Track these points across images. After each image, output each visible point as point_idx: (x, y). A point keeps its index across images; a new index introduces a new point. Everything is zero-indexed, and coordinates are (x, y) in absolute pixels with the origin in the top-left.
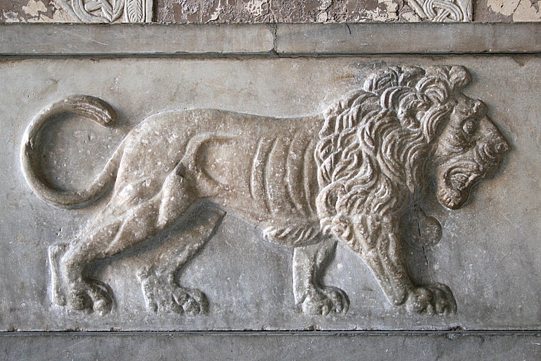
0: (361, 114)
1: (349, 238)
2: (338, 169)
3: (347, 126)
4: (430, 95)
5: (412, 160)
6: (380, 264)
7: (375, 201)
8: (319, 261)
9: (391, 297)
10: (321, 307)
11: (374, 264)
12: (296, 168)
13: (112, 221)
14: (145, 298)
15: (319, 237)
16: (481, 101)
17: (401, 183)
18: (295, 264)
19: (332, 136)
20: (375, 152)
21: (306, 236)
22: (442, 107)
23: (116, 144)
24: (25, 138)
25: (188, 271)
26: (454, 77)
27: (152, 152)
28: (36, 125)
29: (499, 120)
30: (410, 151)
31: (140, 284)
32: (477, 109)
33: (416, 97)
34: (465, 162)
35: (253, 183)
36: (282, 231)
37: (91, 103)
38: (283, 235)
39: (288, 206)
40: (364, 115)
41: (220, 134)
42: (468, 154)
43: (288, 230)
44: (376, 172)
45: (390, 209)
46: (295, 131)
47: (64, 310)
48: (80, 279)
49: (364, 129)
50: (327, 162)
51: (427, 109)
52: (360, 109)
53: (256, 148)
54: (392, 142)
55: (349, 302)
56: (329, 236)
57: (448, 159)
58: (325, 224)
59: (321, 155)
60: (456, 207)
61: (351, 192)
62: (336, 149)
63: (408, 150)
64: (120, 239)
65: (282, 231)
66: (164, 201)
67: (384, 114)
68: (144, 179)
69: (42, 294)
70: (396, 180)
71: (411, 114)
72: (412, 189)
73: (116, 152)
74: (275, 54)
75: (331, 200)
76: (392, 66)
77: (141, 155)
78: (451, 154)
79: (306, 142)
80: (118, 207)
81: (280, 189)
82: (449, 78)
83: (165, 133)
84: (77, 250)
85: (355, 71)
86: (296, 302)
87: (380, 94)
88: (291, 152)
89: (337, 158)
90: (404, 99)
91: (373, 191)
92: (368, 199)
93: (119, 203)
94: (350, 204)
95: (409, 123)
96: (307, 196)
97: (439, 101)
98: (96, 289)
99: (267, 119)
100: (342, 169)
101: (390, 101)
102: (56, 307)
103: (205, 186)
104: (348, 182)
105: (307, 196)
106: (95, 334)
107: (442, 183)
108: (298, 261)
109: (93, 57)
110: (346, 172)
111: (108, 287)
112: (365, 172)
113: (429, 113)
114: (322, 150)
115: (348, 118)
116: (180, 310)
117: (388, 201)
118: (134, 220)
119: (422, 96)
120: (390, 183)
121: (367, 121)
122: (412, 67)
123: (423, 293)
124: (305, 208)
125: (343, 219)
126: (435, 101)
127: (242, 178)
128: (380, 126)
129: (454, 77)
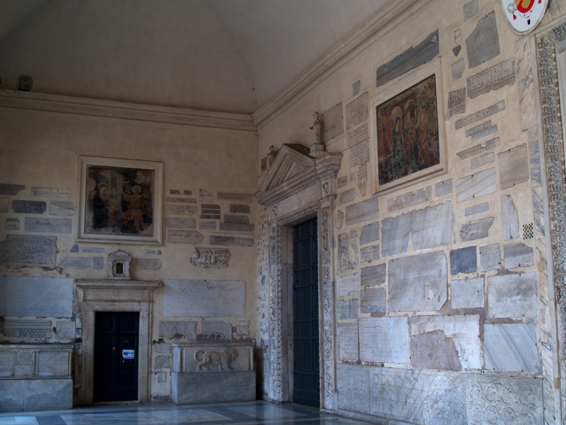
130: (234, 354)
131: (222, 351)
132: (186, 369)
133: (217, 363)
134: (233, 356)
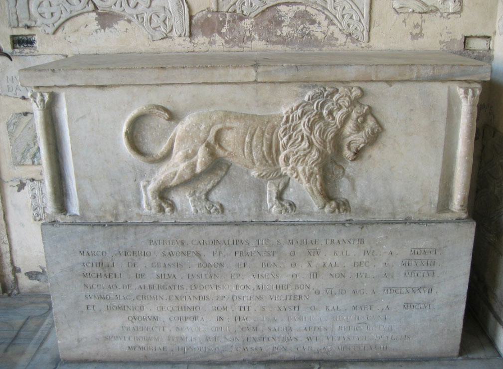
0: (303, 114)
1: (296, 177)
2: (290, 143)
3: (296, 120)
4: (341, 104)
5: (330, 138)
6: (312, 190)
7: (310, 159)
8: (281, 188)
9: (318, 205)
10: (281, 211)
11: (309, 190)
12: (268, 143)
13: (173, 170)
14: (191, 206)
15: (281, 176)
16: (368, 106)
17: (324, 150)
18: (268, 189)
19: (288, 126)
20: (311, 134)
21: (274, 175)
22: (347, 110)
23: (173, 130)
24: (124, 128)
25: (213, 193)
26: (354, 94)
27: (192, 135)
28: (130, 121)
29: (377, 115)
30: (329, 133)
31: (188, 200)
32: (366, 111)
33: (333, 104)
34: (358, 138)
35: (246, 151)
36: (261, 174)
37: (158, 109)
38: (262, 175)
39: (264, 162)
40: (305, 114)
41: (228, 124)
42: (360, 134)
43: (264, 173)
44: (311, 144)
45: (318, 163)
46: (268, 123)
47: (151, 212)
48: (158, 198)
49: (305, 122)
50: (285, 139)
51: (339, 111)
52: (303, 111)
53: (247, 132)
54: (320, 129)
55: (295, 207)
56: (285, 175)
57: (349, 136)
58: (284, 170)
59: (282, 135)
60: (352, 160)
61: (298, 155)
62: (290, 132)
63: (329, 131)
64: (177, 179)
65: (261, 174)
66: (199, 160)
67: (316, 114)
68: (188, 149)
69: (139, 205)
70: (321, 148)
71: (330, 113)
72: (330, 152)
73: (172, 134)
74: (256, 82)
75: (287, 159)
76: (321, 87)
77: (186, 136)
78: (351, 134)
79: (274, 128)
80: (175, 163)
81: (260, 153)
82: (351, 94)
83: (198, 125)
84: (155, 185)
85: (300, 90)
86: (269, 208)
87: (314, 103)
88: (266, 134)
89: (290, 138)
90: (327, 105)
91: (309, 154)
92: (307, 158)
93: (176, 161)
94: (297, 161)
95: (329, 118)
96: (274, 156)
97: (346, 107)
98: (165, 203)
99: (253, 115)
100: (293, 143)
101: (319, 107)
102: (146, 210)
103: (220, 153)
104: (296, 150)
105: (274, 156)
106: (166, 225)
107: (346, 148)
108: (269, 188)
109: (157, 85)
110: (295, 144)
111: (172, 201)
112: (305, 145)
113: (340, 113)
114: (282, 133)
115: (296, 116)
116: (209, 212)
117: (317, 160)
118: (184, 170)
119: (337, 104)
120: (318, 150)
121: (306, 117)
122: (332, 88)
123: (333, 204)
124: (273, 163)
125: (293, 168)
126: (344, 107)
127: (240, 148)
128: (313, 121)
129: (354, 94)
130: (359, 128)
131: (283, 111)
132: (84, 205)
133: (254, 173)
134: (354, 138)
